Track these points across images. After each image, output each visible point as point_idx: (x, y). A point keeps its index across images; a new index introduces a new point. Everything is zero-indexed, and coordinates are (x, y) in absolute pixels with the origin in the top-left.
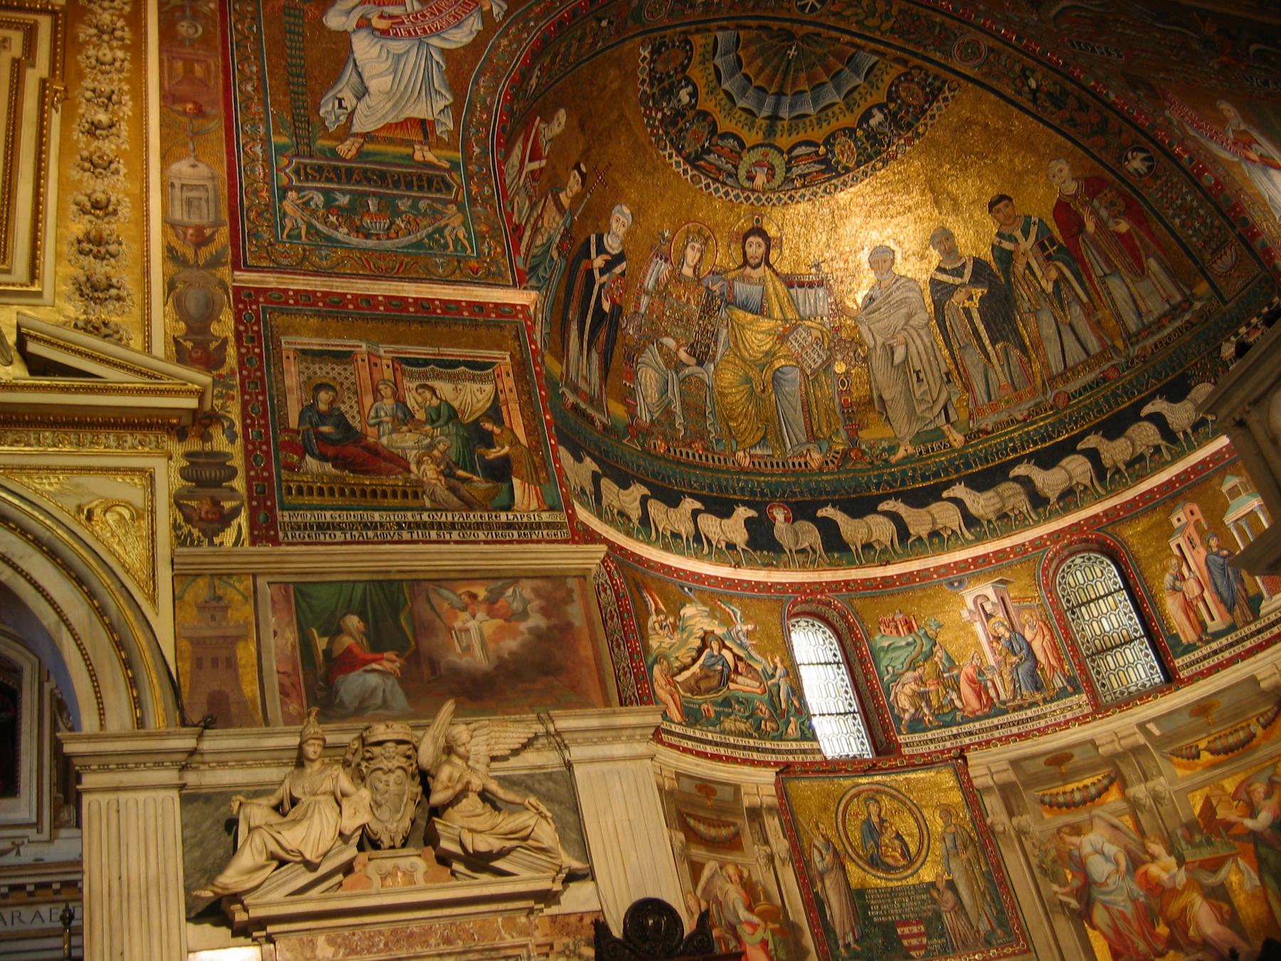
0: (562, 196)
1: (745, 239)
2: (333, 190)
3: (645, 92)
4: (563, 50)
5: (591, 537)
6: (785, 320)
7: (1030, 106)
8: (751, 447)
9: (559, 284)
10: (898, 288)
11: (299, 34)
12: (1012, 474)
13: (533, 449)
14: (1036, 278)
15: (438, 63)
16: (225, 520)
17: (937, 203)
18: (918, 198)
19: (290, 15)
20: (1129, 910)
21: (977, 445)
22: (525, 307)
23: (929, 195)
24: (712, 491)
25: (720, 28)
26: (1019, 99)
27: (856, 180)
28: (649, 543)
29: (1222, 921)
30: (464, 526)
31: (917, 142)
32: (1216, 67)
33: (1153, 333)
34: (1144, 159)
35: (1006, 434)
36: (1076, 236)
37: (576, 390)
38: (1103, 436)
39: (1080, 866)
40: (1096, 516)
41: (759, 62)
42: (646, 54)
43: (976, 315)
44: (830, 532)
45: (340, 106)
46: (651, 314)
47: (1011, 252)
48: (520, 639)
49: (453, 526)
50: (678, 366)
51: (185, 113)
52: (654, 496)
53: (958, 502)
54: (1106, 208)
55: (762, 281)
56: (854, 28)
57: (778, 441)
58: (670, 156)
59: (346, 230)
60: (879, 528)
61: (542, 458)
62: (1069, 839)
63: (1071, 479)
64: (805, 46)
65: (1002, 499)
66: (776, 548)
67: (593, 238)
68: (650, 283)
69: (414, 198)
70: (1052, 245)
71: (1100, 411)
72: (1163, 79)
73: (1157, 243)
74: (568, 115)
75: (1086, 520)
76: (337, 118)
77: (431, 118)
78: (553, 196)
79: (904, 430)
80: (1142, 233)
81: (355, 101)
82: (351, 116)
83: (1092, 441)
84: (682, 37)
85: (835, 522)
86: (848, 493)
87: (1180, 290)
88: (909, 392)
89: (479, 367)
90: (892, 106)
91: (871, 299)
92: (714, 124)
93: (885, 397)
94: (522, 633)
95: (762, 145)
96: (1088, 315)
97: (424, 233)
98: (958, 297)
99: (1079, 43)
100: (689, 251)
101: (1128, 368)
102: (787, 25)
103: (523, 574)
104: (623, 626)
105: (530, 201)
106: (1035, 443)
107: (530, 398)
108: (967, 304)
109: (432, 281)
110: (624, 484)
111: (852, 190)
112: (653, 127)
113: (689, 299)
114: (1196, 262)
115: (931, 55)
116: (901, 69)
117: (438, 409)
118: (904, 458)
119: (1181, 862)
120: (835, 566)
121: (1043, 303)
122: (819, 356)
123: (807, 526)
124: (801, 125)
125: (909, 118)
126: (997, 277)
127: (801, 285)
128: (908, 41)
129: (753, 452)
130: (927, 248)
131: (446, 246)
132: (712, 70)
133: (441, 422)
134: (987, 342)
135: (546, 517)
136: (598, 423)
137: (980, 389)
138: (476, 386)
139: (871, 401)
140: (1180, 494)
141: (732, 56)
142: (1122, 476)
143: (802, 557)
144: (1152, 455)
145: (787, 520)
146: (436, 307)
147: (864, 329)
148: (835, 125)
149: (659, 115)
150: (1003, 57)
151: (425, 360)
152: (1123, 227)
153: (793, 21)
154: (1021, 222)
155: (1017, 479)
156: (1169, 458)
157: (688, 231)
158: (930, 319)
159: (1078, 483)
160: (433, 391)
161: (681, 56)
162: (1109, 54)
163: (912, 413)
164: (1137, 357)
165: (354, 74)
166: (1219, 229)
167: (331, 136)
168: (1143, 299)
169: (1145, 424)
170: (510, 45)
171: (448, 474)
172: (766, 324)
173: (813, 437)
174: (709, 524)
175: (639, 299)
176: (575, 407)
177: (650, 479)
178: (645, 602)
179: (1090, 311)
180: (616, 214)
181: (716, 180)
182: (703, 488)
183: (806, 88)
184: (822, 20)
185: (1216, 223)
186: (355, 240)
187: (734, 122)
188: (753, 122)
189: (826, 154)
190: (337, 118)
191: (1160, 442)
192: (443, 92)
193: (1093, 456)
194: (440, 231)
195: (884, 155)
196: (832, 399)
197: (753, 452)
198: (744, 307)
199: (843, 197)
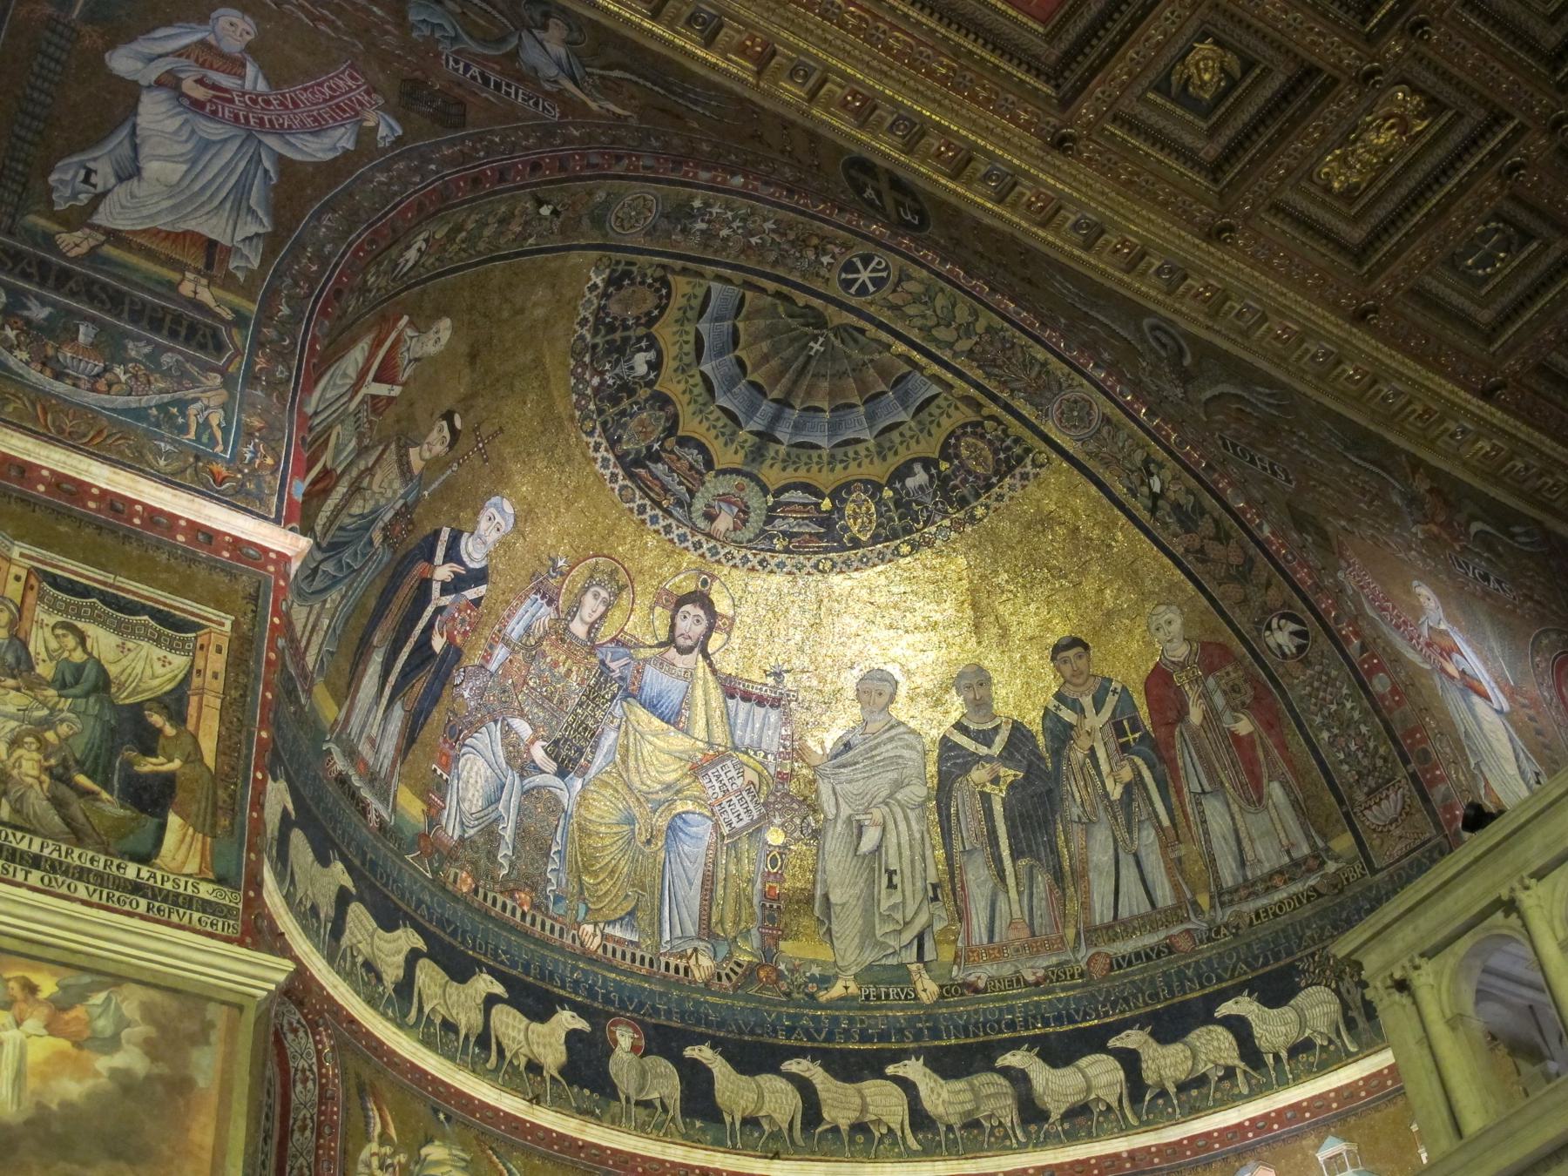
0: (413, 453)
1: (682, 601)
2: (25, 293)
3: (582, 338)
4: (470, 225)
5: (275, 943)
6: (710, 744)
7: (1144, 516)
8: (608, 923)
9: (372, 582)
10: (891, 739)
11: (58, 61)
12: (1000, 1062)
13: (218, 778)
14: (1099, 773)
15: (266, 171)
17: (977, 627)
18: (949, 608)
19: (53, 31)
21: (957, 1004)
22: (283, 558)
23: (969, 612)
24: (527, 972)
25: (718, 278)
26: (1131, 502)
27: (865, 563)
28: (400, 1026)
30: (54, 867)
31: (969, 529)
32: (1420, 536)
33: (1256, 895)
34: (1294, 633)
35: (1004, 999)
36: (1173, 725)
37: (351, 754)
38: (1152, 1034)
40: (1117, 1156)
41: (765, 346)
42: (599, 281)
43: (998, 809)
44: (697, 1082)
45: (86, 180)
46: (504, 676)
47: (1071, 727)
48: (89, 1083)
49: (36, 862)
50: (527, 768)
52: (430, 956)
53: (908, 1086)
54: (1225, 693)
55: (689, 675)
56: (915, 336)
57: (651, 924)
58: (597, 448)
59: (25, 356)
61: (232, 796)
63: (1089, 1089)
64: (837, 343)
66: (605, 1087)
67: (445, 534)
68: (515, 629)
69: (158, 345)
70: (1133, 732)
71: (1155, 996)
72: (1344, 528)
73: (1289, 762)
74: (455, 331)
75: (1098, 1158)
76: (75, 196)
77: (225, 241)
78: (399, 447)
79: (851, 956)
80: (1269, 742)
81: (113, 181)
82: (99, 198)
83: (1132, 1039)
84: (659, 273)
85: (709, 1071)
86: (741, 1032)
87: (1308, 837)
88: (871, 901)
89: (173, 626)
90: (944, 466)
91: (848, 746)
92: (674, 421)
93: (833, 899)
94: (97, 1074)
95: (738, 472)
96: (1165, 847)
97: (155, 399)
98: (978, 774)
99: (1234, 446)
100: (588, 599)
101: (1209, 939)
102: (817, 303)
103: (132, 973)
104: (318, 1147)
105: (360, 442)
106: (1046, 1024)
107: (243, 696)
108: (987, 790)
109: (142, 473)
110: (388, 919)
111: (856, 575)
112: (582, 395)
113: (570, 671)
114: (1341, 802)
115: (1020, 404)
116: (966, 414)
117: (79, 669)
118: (842, 998)
120: (690, 1140)
121: (1102, 813)
122: (748, 811)
123: (664, 1066)
124: (804, 459)
125: (966, 492)
126: (1041, 758)
127: (746, 697)
128: (988, 375)
129: (608, 930)
130: (947, 691)
131: (184, 429)
132: (691, 338)
133: (77, 690)
134: (1006, 853)
135: (206, 891)
136: (372, 816)
137: (979, 920)
138: (158, 652)
139: (810, 900)
140: (1251, 1149)
141: (727, 324)
142: (1168, 1103)
143: (642, 1114)
144: (1221, 1079)
145: (634, 1049)
146: (136, 514)
147: (825, 788)
148: (854, 472)
149: (596, 381)
150: (1122, 435)
151: (86, 587)
152: (1244, 727)
153: (829, 300)
154: (1093, 685)
155: (1006, 1072)
156: (1245, 1091)
157: (595, 569)
158: (928, 799)
159: (1098, 1099)
160: (82, 638)
161: (651, 301)
162: (1274, 473)
163: (867, 936)
164: (1226, 926)
165: (127, 144)
166: (1385, 760)
167: (53, 216)
168: (1252, 841)
169: (1220, 1029)
170: (389, 184)
171: (60, 776)
172: (678, 742)
173: (707, 931)
174: (510, 1024)
175: (491, 647)
176: (342, 780)
177: (432, 928)
178: (367, 1117)
179: (1169, 839)
181: (658, 504)
182: (514, 965)
183: (825, 405)
184: (872, 310)
185: (1382, 751)
186: (35, 375)
187: (706, 424)
188: (734, 433)
189: (830, 512)
190: (75, 196)
191: (1237, 1062)
192: (261, 213)
193: (1130, 1061)
194: (183, 405)
195: (916, 536)
196: (751, 881)
197: (608, 930)
198: (652, 707)
199: (839, 582)
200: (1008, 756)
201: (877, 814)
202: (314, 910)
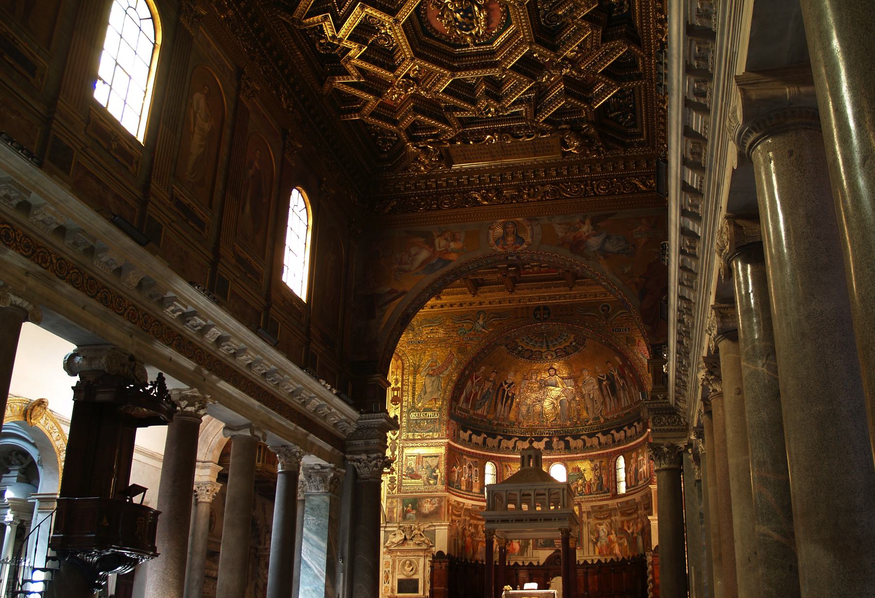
0: (490, 379)
16: (394, 488)
20: (605, 544)
29: (620, 551)
39: (598, 532)
44: (567, 444)
51: (393, 404)
60: (580, 443)
62: (598, 526)
65: (608, 439)
67: (503, 382)
83: (626, 428)
88: (593, 406)
98: (604, 383)
100: (533, 377)
119: (616, 536)
137: (608, 408)
147: (583, 389)
171: (428, 479)
172: (558, 389)
176: (497, 424)
179: (629, 392)
180: (509, 375)
193: (625, 431)
200: (606, 380)
201: (592, 392)
202: (494, 447)
